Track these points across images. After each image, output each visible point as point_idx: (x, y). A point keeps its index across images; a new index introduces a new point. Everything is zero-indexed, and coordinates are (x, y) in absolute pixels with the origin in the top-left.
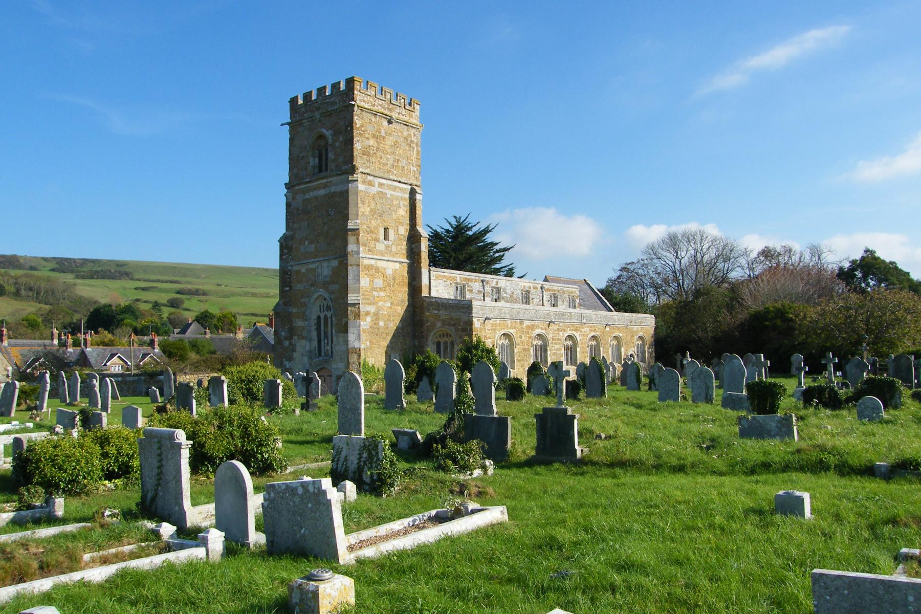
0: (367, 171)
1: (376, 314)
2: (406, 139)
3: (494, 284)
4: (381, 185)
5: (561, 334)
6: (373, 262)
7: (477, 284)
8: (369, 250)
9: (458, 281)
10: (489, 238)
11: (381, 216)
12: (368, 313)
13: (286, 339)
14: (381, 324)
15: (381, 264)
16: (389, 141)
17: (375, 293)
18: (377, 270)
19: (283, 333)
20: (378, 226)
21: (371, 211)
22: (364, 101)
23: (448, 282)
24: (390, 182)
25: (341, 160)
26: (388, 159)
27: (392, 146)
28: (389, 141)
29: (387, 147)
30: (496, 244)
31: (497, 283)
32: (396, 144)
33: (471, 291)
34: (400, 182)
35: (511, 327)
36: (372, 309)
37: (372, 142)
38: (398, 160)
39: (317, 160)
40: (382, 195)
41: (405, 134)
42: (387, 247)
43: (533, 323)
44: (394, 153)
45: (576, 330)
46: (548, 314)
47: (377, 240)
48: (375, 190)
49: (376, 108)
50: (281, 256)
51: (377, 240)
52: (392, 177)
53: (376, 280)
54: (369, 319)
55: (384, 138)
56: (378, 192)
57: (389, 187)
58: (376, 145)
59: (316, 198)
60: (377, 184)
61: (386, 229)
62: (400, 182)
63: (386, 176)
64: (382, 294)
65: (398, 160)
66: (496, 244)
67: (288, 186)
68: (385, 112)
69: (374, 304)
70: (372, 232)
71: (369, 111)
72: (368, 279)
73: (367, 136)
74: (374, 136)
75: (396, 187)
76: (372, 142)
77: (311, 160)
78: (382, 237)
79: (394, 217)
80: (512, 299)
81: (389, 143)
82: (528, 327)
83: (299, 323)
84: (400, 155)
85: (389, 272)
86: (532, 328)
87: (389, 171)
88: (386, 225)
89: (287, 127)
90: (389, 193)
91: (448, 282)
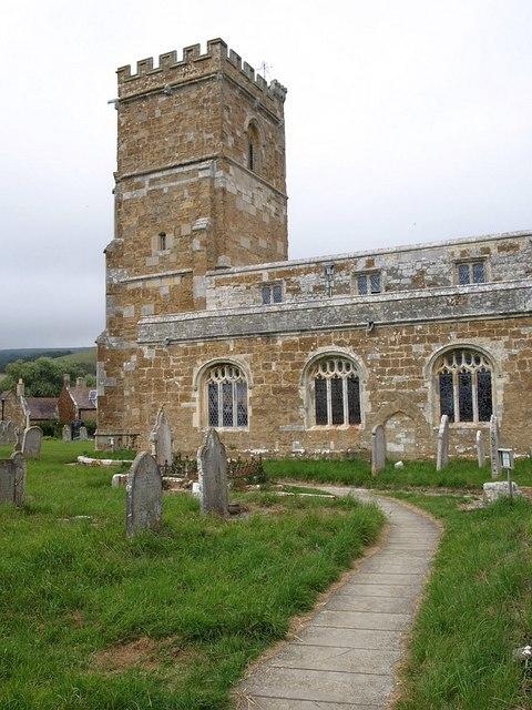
2: (195, 101)
4: (152, 182)
5: (418, 348)
6: (140, 284)
7: (312, 276)
9: (265, 279)
15: (149, 284)
18: (146, 292)
20: (150, 235)
24: (165, 173)
32: (179, 118)
33: (296, 291)
34: (181, 165)
35: (240, 350)
37: (143, 133)
46: (362, 311)
48: (147, 188)
51: (149, 254)
56: (149, 193)
60: (147, 183)
62: (181, 165)
63: (164, 165)
70: (141, 246)
78: (155, 248)
85: (165, 291)
86: (306, 345)
87: (167, 159)
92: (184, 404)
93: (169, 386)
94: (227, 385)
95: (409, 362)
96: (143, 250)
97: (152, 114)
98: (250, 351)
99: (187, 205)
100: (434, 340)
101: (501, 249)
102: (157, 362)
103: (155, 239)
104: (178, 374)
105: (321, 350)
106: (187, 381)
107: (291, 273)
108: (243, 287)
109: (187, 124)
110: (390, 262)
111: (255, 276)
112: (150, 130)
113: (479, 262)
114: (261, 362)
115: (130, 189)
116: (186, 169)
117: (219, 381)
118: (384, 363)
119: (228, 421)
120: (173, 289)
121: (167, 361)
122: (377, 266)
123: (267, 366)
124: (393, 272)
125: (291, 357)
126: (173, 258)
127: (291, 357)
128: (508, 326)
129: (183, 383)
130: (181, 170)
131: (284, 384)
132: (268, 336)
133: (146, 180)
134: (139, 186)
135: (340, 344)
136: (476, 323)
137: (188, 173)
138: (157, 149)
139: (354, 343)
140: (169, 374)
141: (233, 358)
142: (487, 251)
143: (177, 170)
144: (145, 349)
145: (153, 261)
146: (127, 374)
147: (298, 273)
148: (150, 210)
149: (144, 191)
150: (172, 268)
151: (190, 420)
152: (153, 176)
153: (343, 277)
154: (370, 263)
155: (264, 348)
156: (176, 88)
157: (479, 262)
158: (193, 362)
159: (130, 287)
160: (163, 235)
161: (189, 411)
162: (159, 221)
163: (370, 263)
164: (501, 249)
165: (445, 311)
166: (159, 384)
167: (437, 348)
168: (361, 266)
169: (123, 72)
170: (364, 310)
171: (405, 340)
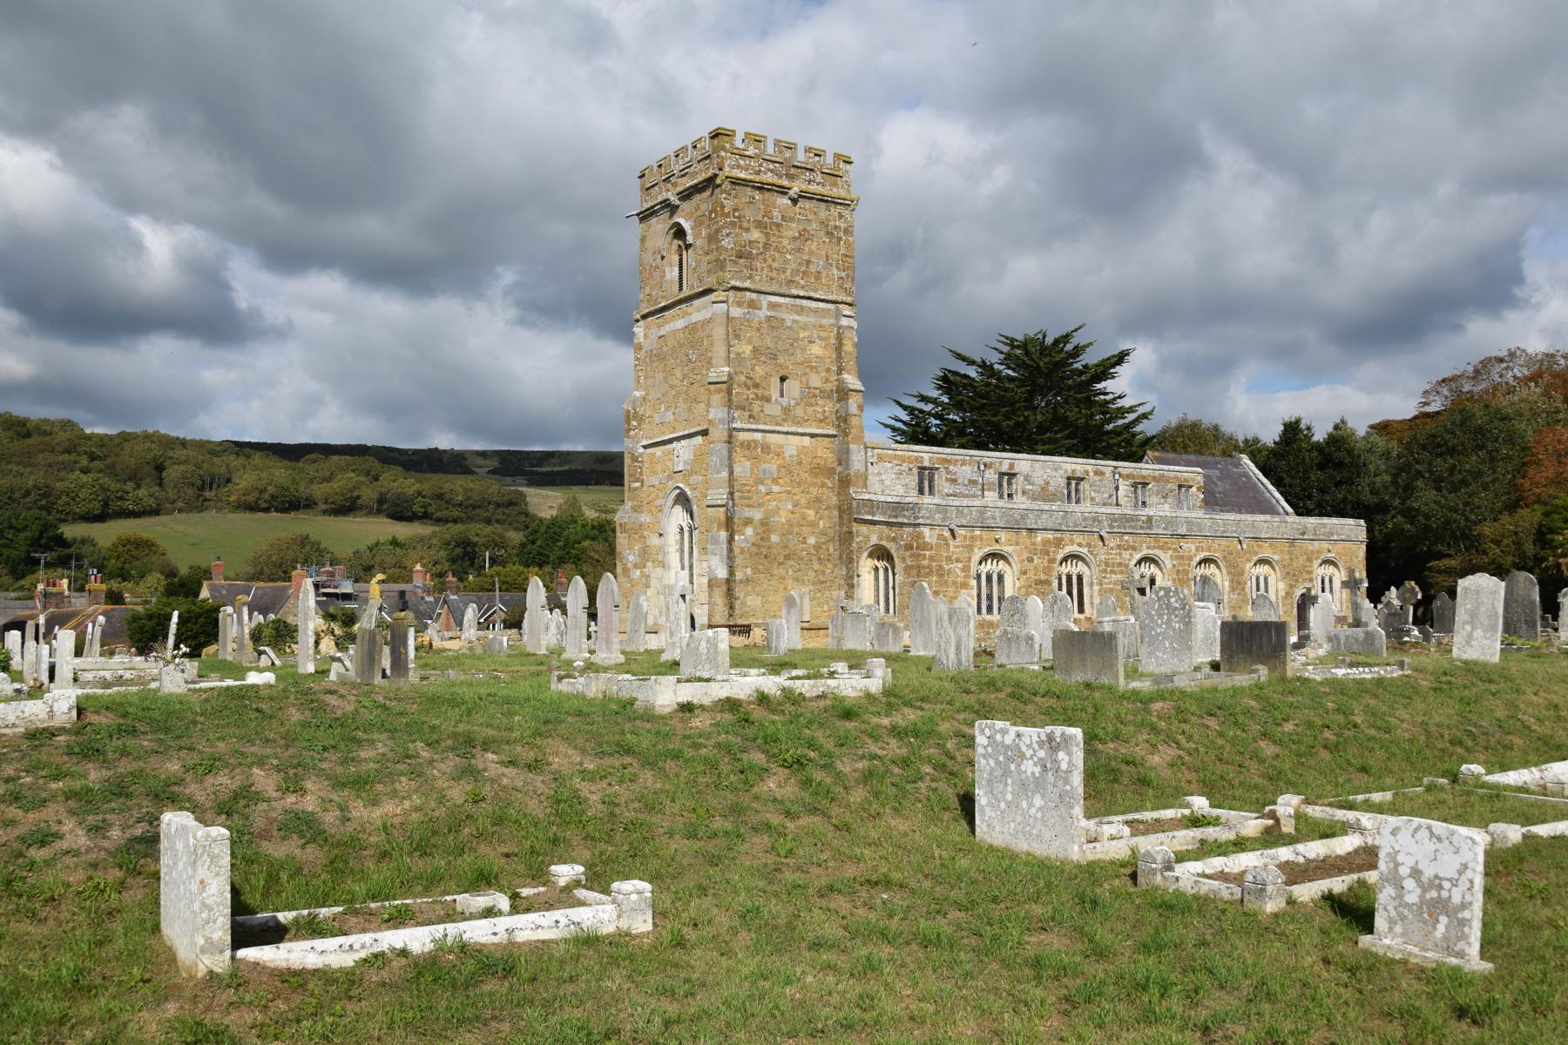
0: (747, 284)
1: (765, 523)
3: (1005, 468)
4: (772, 306)
5: (1126, 554)
6: (758, 436)
7: (966, 468)
8: (751, 417)
9: (926, 464)
11: (775, 357)
12: (748, 522)
13: (636, 566)
14: (774, 538)
16: (792, 230)
17: (762, 488)
18: (766, 448)
19: (631, 558)
21: (755, 350)
22: (738, 166)
23: (905, 467)
25: (704, 268)
26: (786, 261)
27: (795, 238)
28: (792, 230)
29: (785, 242)
31: (1011, 466)
32: (804, 236)
33: (954, 481)
36: (757, 515)
37: (755, 234)
38: (808, 262)
39: (676, 269)
40: (774, 323)
41: (823, 214)
42: (787, 410)
43: (1058, 535)
44: (799, 250)
45: (1161, 548)
46: (1095, 519)
47: (768, 400)
48: (764, 313)
51: (768, 400)
52: (794, 292)
54: (749, 531)
55: (778, 226)
56: (769, 318)
58: (763, 239)
59: (675, 332)
60: (765, 304)
61: (783, 379)
64: (776, 489)
65: (808, 262)
68: (780, 182)
69: (760, 505)
70: (757, 386)
71: (744, 183)
73: (745, 225)
74: (759, 225)
77: (667, 270)
78: (775, 395)
79: (799, 357)
80: (1045, 494)
81: (790, 233)
82: (1046, 542)
83: (654, 540)
84: (811, 253)
86: (1058, 543)
88: (783, 373)
90: (789, 318)
91: (905, 467)
93: (949, 572)
95: (1120, 565)
96: (760, 392)
97: (768, 214)
98: (1017, 544)
99: (816, 350)
100: (1134, 548)
101: (1096, 473)
102: (938, 546)
103: (775, 381)
104: (958, 560)
105: (1069, 549)
106: (966, 569)
109: (813, 247)
112: (767, 235)
114: (1025, 555)
115: (740, 304)
116: (814, 304)
120: (802, 450)
122: (1016, 470)
123: (1030, 560)
124: (1027, 478)
125: (1047, 553)
126: (799, 412)
127: (1047, 553)
129: (963, 570)
131: (1043, 577)
133: (765, 300)
135: (1080, 545)
137: (816, 311)
138: (775, 265)
139: (1089, 545)
140: (949, 559)
141: (1007, 549)
142: (1087, 472)
143: (805, 303)
145: (773, 410)
148: (768, 342)
150: (799, 424)
156: (803, 196)
158: (970, 548)
160: (783, 379)
162: (781, 360)
164: (1096, 473)
167: (1138, 556)
171: (1119, 547)
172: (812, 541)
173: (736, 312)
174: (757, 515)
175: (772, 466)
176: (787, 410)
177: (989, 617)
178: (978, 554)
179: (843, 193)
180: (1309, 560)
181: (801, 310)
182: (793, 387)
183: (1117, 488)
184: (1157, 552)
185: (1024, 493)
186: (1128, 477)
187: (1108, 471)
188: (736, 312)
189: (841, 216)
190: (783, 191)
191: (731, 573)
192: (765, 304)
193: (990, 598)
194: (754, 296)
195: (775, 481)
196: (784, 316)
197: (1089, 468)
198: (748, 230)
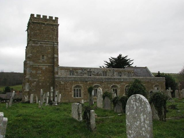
1: (38, 82)
2: (52, 29)
4: (41, 43)
5: (109, 85)
7: (80, 70)
9: (71, 70)
10: (127, 58)
12: (35, 81)
18: (39, 68)
24: (45, 42)
29: (44, 32)
30: (129, 59)
33: (77, 73)
34: (49, 42)
37: (38, 31)
44: (47, 34)
46: (101, 79)
47: (40, 60)
49: (40, 22)
50: (24, 66)
51: (40, 60)
52: (45, 41)
53: (38, 71)
54: (35, 83)
55: (43, 30)
56: (40, 46)
57: (44, 44)
60: (39, 43)
61: (43, 56)
62: (49, 42)
64: (40, 75)
65: (48, 36)
66: (129, 59)
67: (26, 47)
70: (37, 57)
71: (36, 23)
72: (35, 71)
74: (39, 30)
75: (47, 43)
76: (38, 31)
82: (90, 83)
84: (49, 34)
85: (44, 68)
86: (93, 84)
89: (27, 31)
92: (70, 93)
94: (77, 90)
95: (108, 87)
96: (38, 58)
99: (50, 51)
101: (109, 71)
103: (41, 56)
105: (95, 85)
106: (71, 89)
107: (76, 69)
108: (66, 70)
110: (93, 70)
111: (69, 69)
113: (106, 72)
115: (34, 43)
116: (49, 43)
117: (76, 89)
118: (104, 87)
119: (77, 96)
121: (67, 85)
122: (91, 70)
123: (86, 87)
124: (94, 72)
126: (46, 62)
128: (120, 83)
130: (51, 43)
132: (86, 82)
134: (37, 43)
135: (98, 84)
136: (116, 82)
139: (100, 84)
140: (67, 87)
141: (80, 85)
144: (62, 82)
146: (33, 86)
147: (78, 69)
149: (38, 45)
151: (71, 96)
152: (41, 42)
153: (85, 72)
154: (90, 70)
155: (86, 83)
156: (47, 24)
157: (106, 72)
159: (34, 66)
160: (43, 56)
161: (71, 94)
163: (90, 70)
165: (113, 80)
166: (65, 89)
168: (89, 70)
169: (32, 15)
170: (102, 78)
171: (107, 84)
172: (48, 84)
173: (33, 45)
174: (37, 80)
175: (40, 72)
176: (43, 61)
177: (77, 98)
178: (73, 86)
179: (56, 24)
180: (152, 85)
181: (47, 44)
182: (45, 57)
183: (114, 73)
184: (116, 85)
185: (93, 74)
186: (116, 71)
187: (112, 70)
188: (33, 45)
189: (56, 27)
190: (44, 24)
191: (30, 90)
192: (39, 43)
193: (77, 94)
194: (37, 42)
195: (40, 74)
196: (43, 45)
197: (108, 70)
198: (36, 31)
